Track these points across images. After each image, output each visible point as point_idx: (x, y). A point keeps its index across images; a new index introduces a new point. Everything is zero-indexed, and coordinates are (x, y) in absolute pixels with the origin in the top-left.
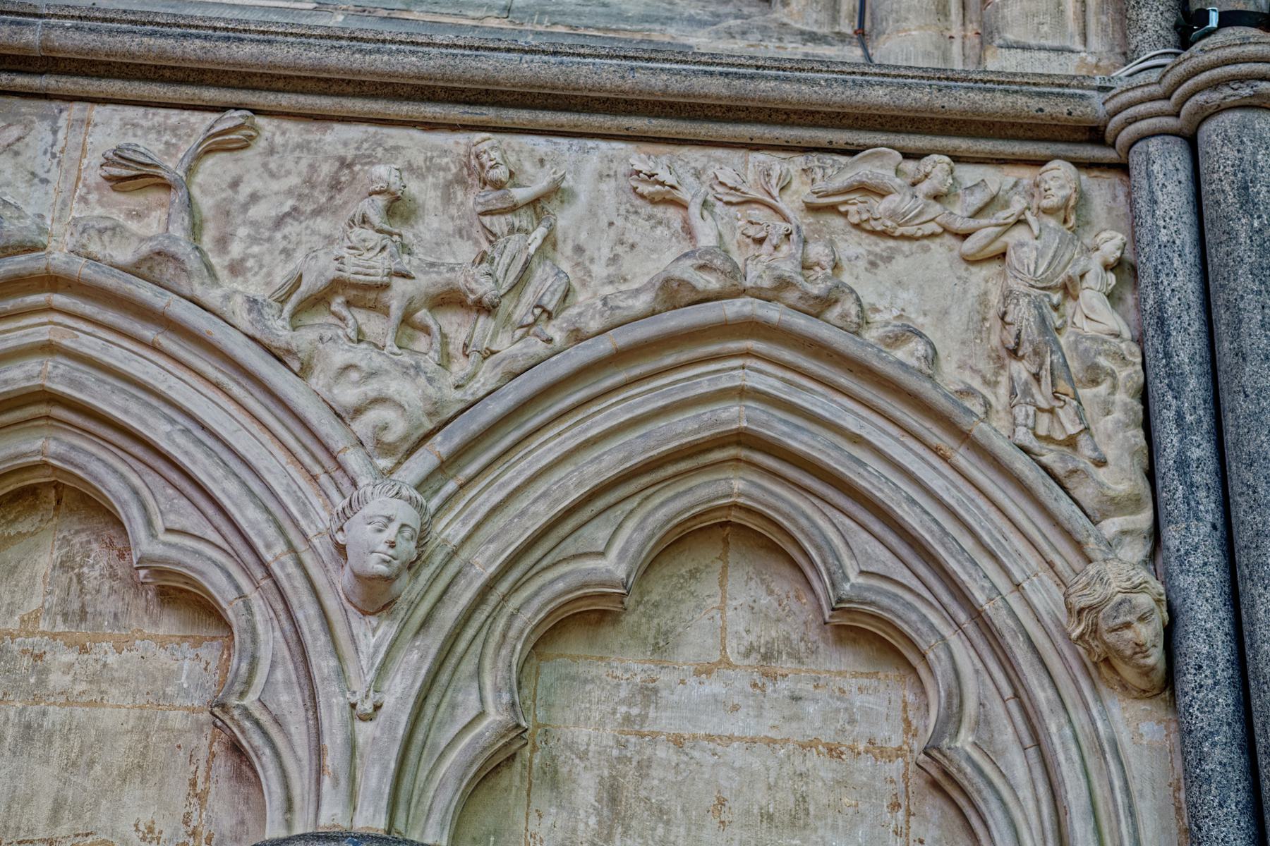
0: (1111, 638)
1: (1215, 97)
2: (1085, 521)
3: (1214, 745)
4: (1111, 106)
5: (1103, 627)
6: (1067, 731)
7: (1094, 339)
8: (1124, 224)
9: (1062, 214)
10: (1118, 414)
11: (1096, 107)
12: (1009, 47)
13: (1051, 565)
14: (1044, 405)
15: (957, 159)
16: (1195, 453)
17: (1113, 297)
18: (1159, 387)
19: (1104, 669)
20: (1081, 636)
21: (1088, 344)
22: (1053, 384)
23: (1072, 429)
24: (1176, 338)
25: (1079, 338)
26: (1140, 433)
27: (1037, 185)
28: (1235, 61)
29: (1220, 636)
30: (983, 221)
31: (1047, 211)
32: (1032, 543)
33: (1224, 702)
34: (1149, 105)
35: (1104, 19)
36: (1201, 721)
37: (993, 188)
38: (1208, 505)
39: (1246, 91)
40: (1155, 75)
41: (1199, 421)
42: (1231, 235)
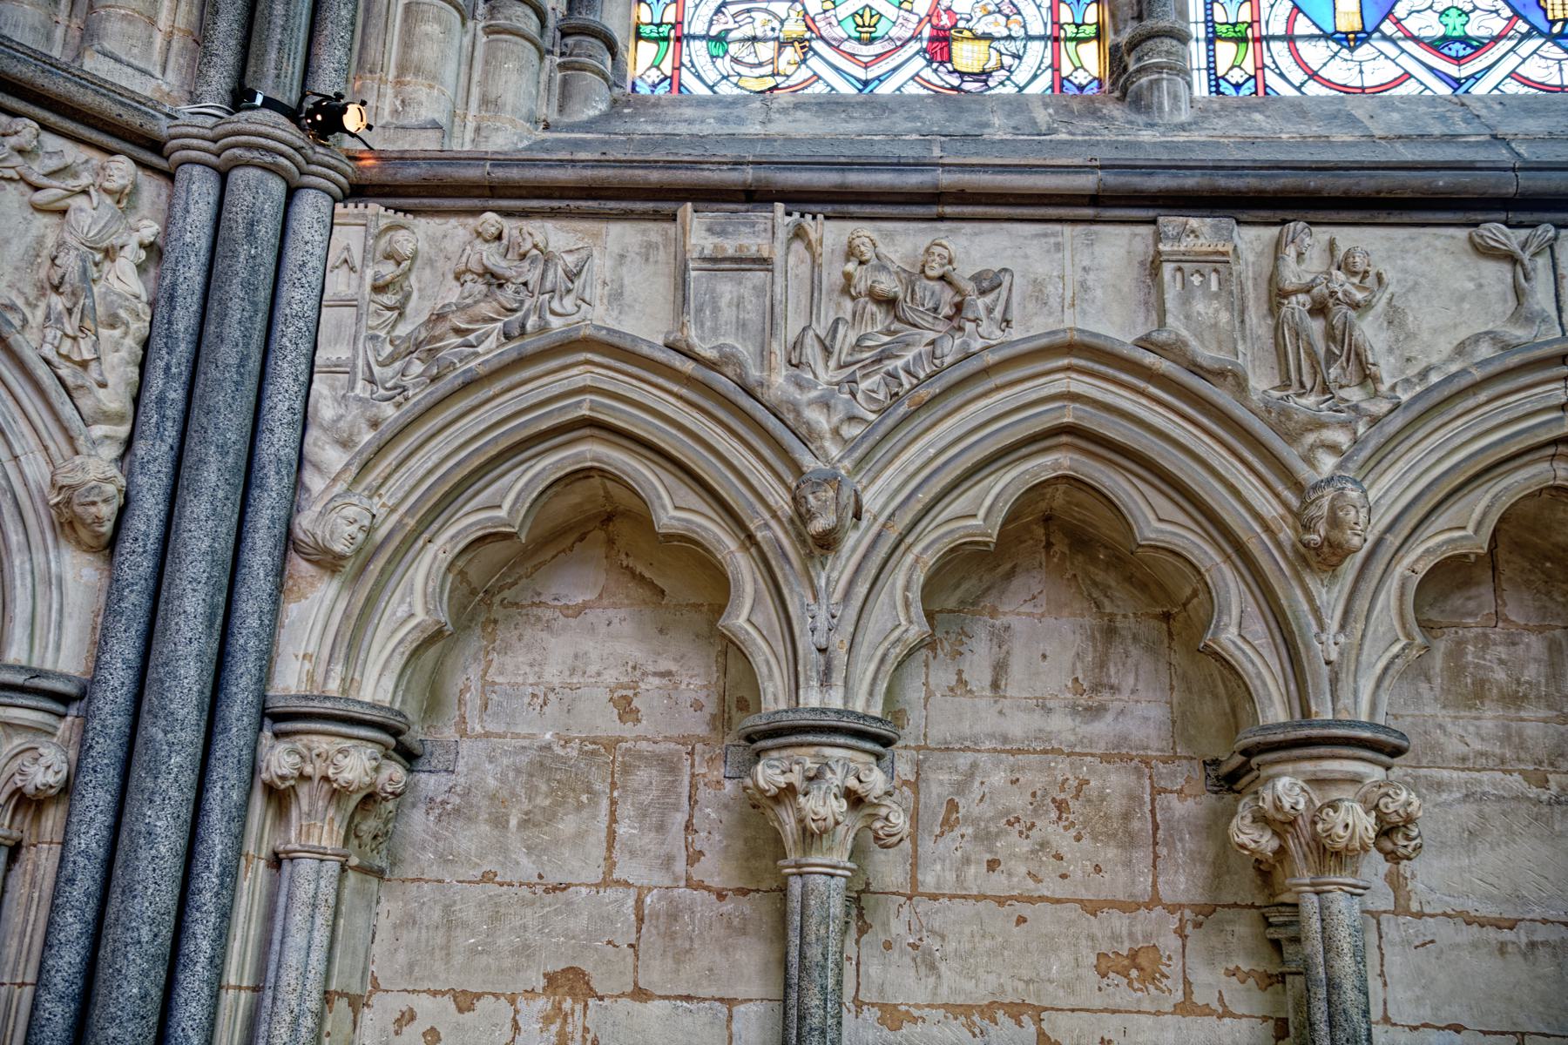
0: (79, 510)
1: (248, 155)
2: (80, 423)
3: (132, 591)
4: (173, 131)
5: (76, 500)
6: (27, 566)
7: (119, 295)
8: (161, 217)
9: (117, 196)
10: (123, 353)
11: (162, 127)
12: (105, 55)
13: (46, 448)
14: (69, 331)
15: (44, 127)
16: (172, 395)
17: (141, 268)
18: (158, 342)
19: (67, 528)
20: (57, 504)
21: (115, 298)
22: (81, 320)
23: (87, 356)
24: (179, 312)
25: (109, 291)
26: (137, 370)
27: (103, 168)
28: (267, 136)
29: (156, 521)
30: (55, 183)
31: (106, 191)
32: (35, 430)
33: (146, 565)
34: (200, 141)
35: (181, 61)
36: (128, 574)
37: (69, 160)
38: (171, 432)
39: (269, 159)
40: (211, 121)
41: (181, 374)
42: (235, 254)
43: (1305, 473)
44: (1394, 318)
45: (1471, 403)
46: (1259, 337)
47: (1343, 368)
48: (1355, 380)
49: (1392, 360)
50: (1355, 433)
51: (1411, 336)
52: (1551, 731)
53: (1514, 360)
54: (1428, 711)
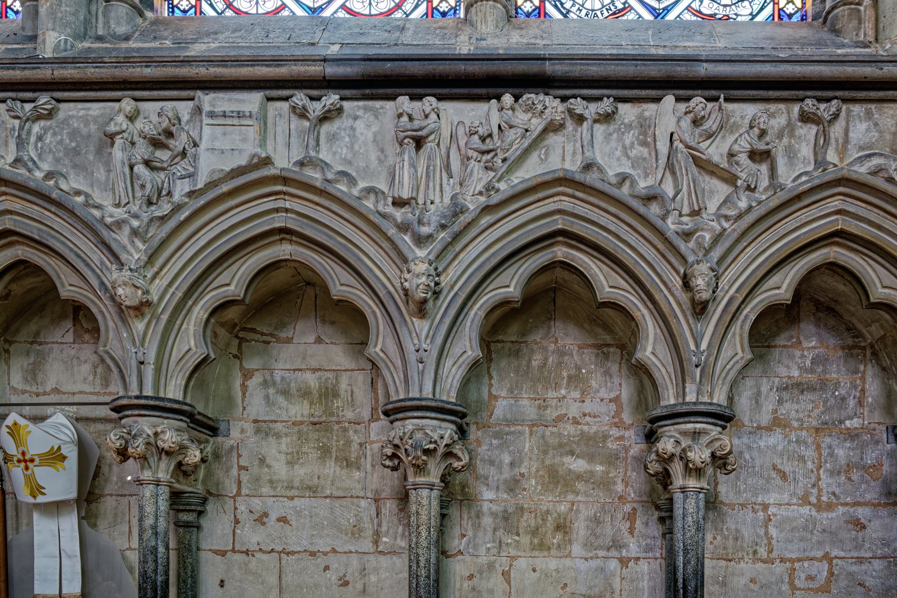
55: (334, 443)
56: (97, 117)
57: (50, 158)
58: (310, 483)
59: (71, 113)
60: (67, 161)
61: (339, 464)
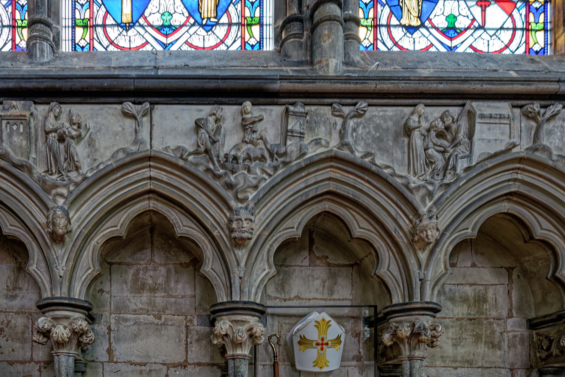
43: (51, 204)
44: (91, 143)
45: (114, 177)
46: (42, 152)
47: (69, 164)
48: (74, 168)
49: (89, 160)
50: (69, 189)
51: (96, 150)
52: (164, 300)
53: (128, 159)
54: (125, 294)
55: (484, 332)
56: (392, 116)
57: (362, 143)
58: (468, 359)
59: (374, 114)
60: (374, 146)
61: (487, 345)
